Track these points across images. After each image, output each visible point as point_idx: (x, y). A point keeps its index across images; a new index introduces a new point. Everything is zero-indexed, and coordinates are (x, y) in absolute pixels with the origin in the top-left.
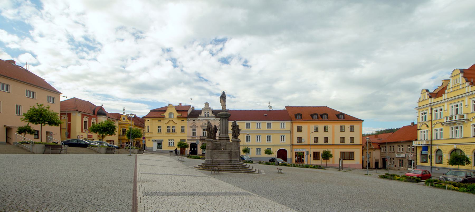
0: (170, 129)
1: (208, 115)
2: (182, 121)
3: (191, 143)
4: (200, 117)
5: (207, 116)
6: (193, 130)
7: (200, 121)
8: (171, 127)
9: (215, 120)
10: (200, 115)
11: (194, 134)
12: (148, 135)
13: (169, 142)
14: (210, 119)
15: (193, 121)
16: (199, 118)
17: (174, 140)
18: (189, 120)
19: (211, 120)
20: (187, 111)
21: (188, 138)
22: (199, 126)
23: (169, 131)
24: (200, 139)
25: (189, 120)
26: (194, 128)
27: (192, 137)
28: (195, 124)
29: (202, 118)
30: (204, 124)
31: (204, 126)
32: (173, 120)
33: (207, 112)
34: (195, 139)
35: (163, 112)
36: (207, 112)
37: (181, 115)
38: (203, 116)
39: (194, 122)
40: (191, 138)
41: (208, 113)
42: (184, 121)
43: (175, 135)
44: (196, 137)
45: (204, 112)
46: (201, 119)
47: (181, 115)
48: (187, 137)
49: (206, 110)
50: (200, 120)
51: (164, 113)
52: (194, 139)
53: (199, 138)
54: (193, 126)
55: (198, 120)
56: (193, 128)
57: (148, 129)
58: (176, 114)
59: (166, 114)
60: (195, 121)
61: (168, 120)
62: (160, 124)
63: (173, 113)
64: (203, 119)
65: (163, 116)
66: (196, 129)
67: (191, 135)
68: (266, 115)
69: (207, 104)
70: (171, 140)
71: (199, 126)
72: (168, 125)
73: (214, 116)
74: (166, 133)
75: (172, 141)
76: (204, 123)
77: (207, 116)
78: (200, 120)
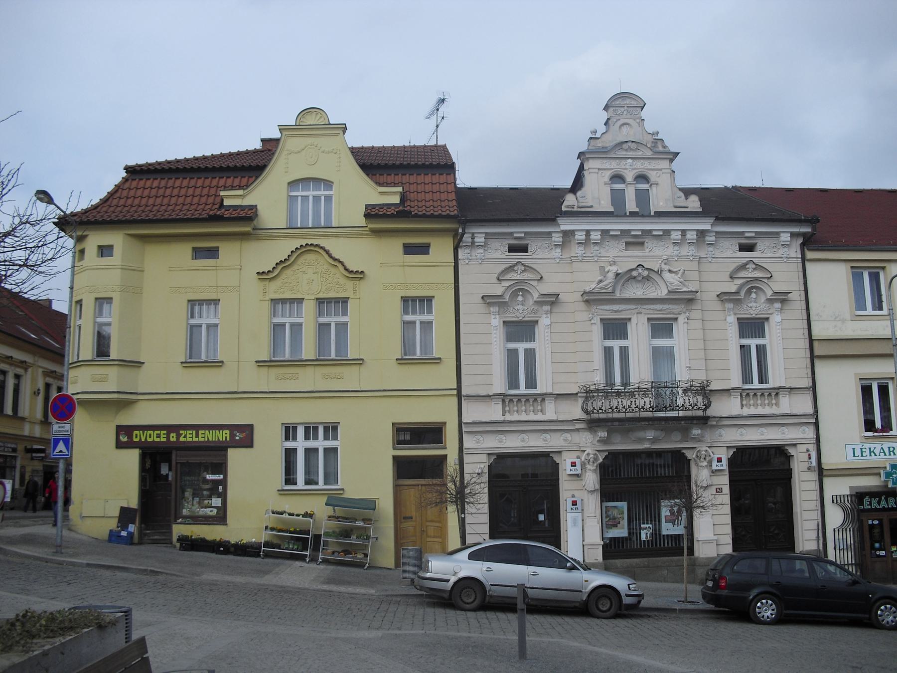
0: (297, 328)
1: (643, 198)
2: (409, 249)
5: (631, 205)
7: (576, 251)
8: (309, 308)
9: (711, 238)
12: (102, 380)
13: (290, 454)
14: (667, 233)
15: (512, 249)
16: (566, 225)
17: (331, 430)
18: (480, 239)
21: (472, 412)
22: (571, 297)
24: (583, 416)
25: (480, 239)
26: (520, 311)
27: (505, 399)
29: (597, 226)
30: (611, 276)
31: (618, 295)
33: (629, 177)
36: (629, 177)
37: (403, 199)
38: (596, 209)
40: (494, 412)
41: (642, 178)
42: (424, 249)
43: (350, 378)
44: (544, 396)
45: (607, 175)
46: (588, 233)
47: (396, 200)
48: (459, 396)
49: (622, 153)
53: (574, 410)
54: (515, 294)
55: (557, 238)
56: (510, 317)
60: (524, 249)
63: (328, 184)
64: (605, 233)
65: (235, 207)
66: (544, 321)
67: (499, 385)
70: (311, 431)
71: (571, 297)
74: (260, 363)
75: (321, 444)
76: (614, 269)
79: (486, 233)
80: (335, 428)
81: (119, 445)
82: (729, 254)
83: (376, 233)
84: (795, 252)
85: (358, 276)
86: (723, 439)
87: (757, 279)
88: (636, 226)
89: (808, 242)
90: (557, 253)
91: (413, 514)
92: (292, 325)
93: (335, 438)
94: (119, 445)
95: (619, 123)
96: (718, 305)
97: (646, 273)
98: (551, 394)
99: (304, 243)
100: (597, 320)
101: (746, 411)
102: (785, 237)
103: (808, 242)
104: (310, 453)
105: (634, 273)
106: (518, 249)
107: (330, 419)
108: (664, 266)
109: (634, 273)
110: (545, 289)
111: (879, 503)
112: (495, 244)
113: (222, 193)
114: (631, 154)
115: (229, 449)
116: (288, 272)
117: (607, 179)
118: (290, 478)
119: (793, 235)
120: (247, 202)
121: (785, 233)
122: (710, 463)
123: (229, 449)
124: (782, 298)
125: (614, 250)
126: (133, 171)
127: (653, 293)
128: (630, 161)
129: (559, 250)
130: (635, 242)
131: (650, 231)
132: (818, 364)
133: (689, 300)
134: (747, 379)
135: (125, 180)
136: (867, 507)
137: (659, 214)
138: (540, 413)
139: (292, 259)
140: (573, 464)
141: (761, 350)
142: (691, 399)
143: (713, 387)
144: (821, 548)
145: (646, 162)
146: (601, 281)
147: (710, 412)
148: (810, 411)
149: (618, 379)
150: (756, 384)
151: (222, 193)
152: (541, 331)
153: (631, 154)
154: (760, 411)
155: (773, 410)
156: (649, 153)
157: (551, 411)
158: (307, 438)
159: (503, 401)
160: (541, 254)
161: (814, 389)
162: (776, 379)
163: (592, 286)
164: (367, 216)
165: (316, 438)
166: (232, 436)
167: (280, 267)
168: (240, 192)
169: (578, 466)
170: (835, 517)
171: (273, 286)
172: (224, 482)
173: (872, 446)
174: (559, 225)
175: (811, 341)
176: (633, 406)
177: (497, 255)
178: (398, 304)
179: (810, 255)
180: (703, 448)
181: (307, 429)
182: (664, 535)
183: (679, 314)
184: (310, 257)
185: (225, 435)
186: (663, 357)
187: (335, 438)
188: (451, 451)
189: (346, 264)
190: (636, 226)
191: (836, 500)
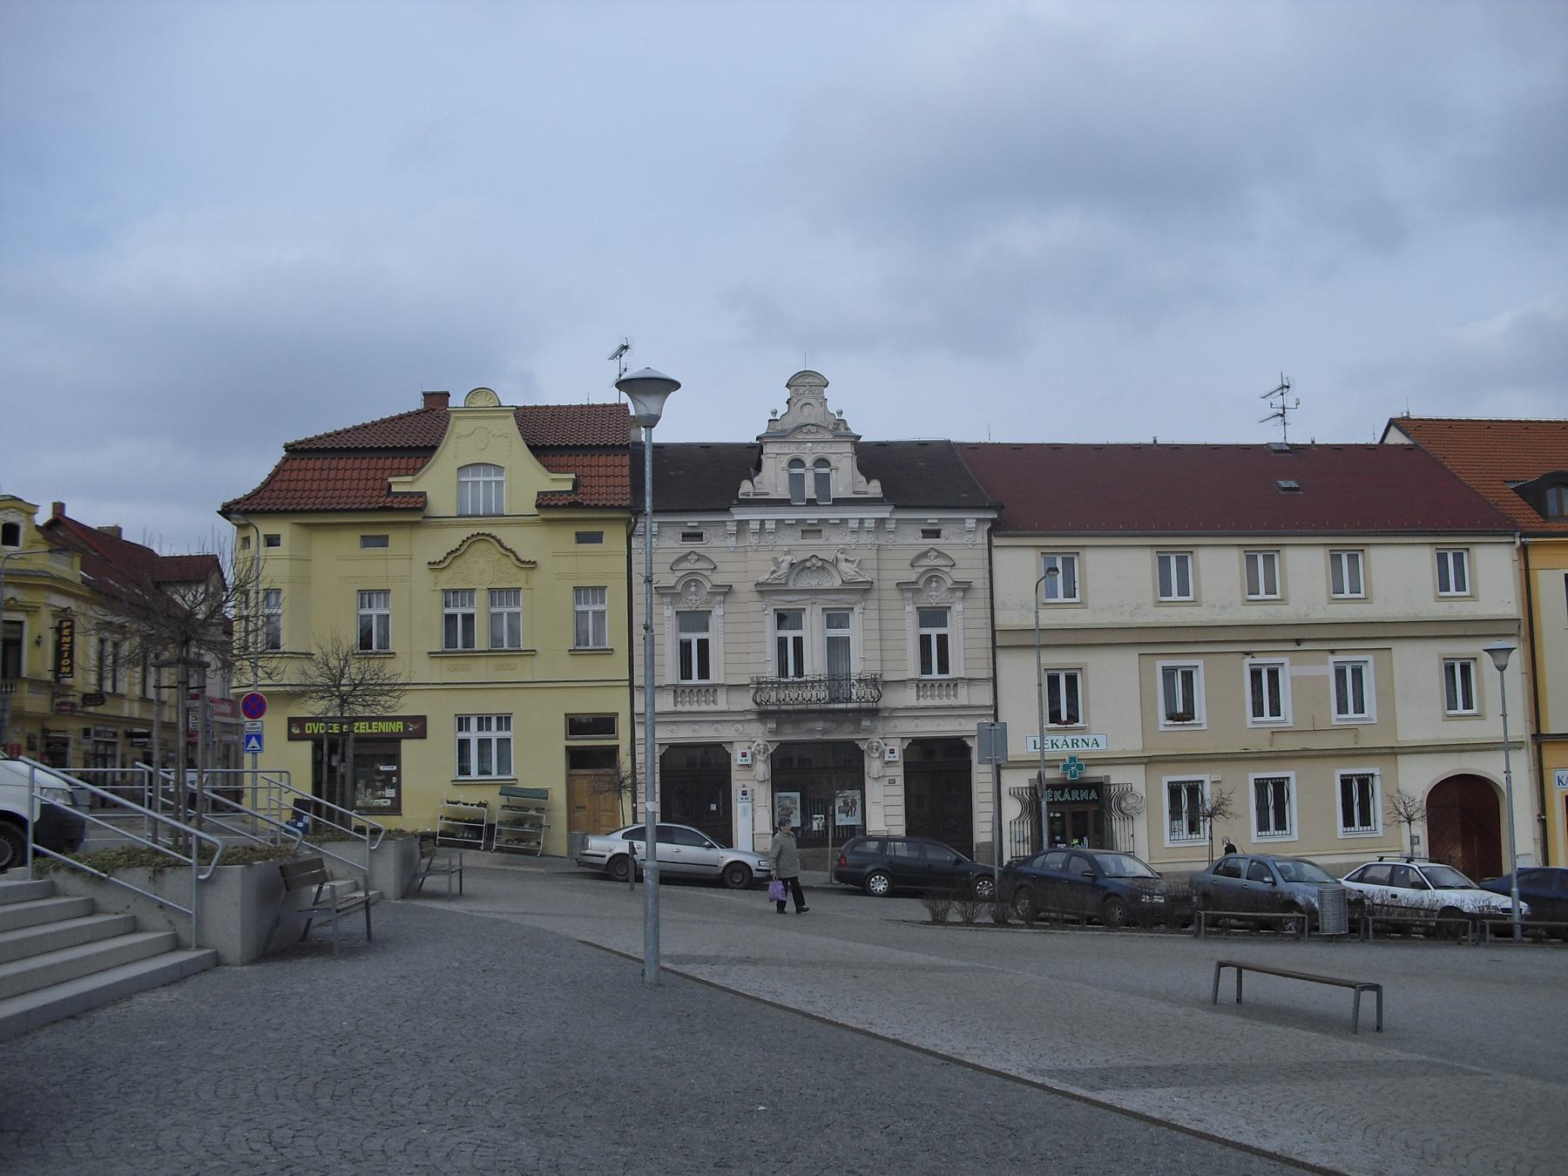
0: (468, 619)
1: (822, 482)
2: (582, 538)
3: (672, 747)
5: (810, 493)
6: (683, 629)
8: (481, 598)
9: (891, 526)
10: (746, 487)
11: (695, 658)
13: (463, 745)
14: (844, 521)
15: (686, 536)
16: (739, 514)
17: (504, 721)
19: (854, 524)
22: (744, 588)
28: (699, 565)
29: (771, 515)
30: (785, 566)
31: (791, 586)
32: (494, 531)
33: (809, 463)
34: (704, 707)
36: (809, 463)
37: (576, 484)
39: (691, 545)
41: (822, 462)
42: (596, 538)
43: (522, 670)
44: (715, 687)
45: (785, 460)
46: (762, 522)
47: (569, 487)
48: (631, 686)
49: (800, 437)
50: (755, 526)
51: (414, 471)
52: (695, 708)
53: (745, 702)
54: (687, 585)
55: (732, 528)
56: (683, 608)
60: (699, 536)
62: (373, 567)
63: (499, 469)
64: (779, 522)
65: (404, 494)
66: (718, 611)
68: (1293, 484)
69: (806, 384)
70: (484, 722)
71: (744, 588)
72: (451, 579)
73: (875, 489)
75: (494, 734)
76: (789, 558)
79: (659, 523)
80: (508, 719)
81: (292, 737)
82: (911, 540)
83: (546, 521)
84: (981, 538)
85: (531, 565)
86: (897, 730)
87: (935, 569)
88: (812, 515)
89: (996, 529)
90: (732, 541)
91: (587, 804)
92: (464, 616)
93: (508, 728)
94: (292, 737)
95: (801, 403)
96: (896, 595)
97: (820, 564)
98: (723, 685)
100: (770, 611)
101: (923, 703)
102: (971, 524)
103: (996, 529)
104: (484, 744)
105: (808, 564)
106: (693, 536)
108: (839, 555)
109: (808, 564)
110: (718, 579)
111: (1062, 796)
112: (668, 532)
113: (390, 480)
114: (810, 437)
115: (402, 741)
116: (460, 561)
117: (785, 464)
118: (464, 770)
119: (979, 520)
120: (415, 489)
121: (970, 519)
122: (882, 754)
123: (402, 741)
124: (965, 588)
125: (791, 539)
126: (294, 450)
127: (827, 585)
128: (809, 445)
129: (733, 539)
130: (811, 530)
132: (998, 652)
133: (865, 590)
135: (285, 460)
137: (839, 502)
138: (712, 704)
139: (463, 549)
140: (744, 755)
141: (942, 640)
142: (868, 692)
143: (888, 677)
145: (827, 445)
146: (774, 572)
147: (881, 704)
148: (989, 701)
149: (791, 671)
151: (390, 480)
152: (715, 622)
154: (937, 702)
155: (952, 702)
156: (829, 437)
157: (723, 702)
158: (480, 728)
159: (675, 691)
160: (715, 542)
161: (994, 680)
162: (956, 670)
163: (763, 578)
164: (538, 506)
165: (489, 729)
166: (406, 727)
167: (451, 557)
168: (409, 479)
169: (749, 757)
170: (1012, 809)
171: (444, 576)
172: (398, 773)
173: (1055, 738)
174: (732, 515)
175: (994, 631)
176: (800, 698)
177: (671, 544)
178: (571, 594)
179: (996, 541)
180: (875, 739)
181: (480, 720)
182: (838, 826)
183: (854, 604)
184: (481, 546)
185: (397, 727)
186: (837, 649)
187: (508, 728)
188: (623, 743)
189: (518, 554)
190: (812, 515)
191: (1016, 793)
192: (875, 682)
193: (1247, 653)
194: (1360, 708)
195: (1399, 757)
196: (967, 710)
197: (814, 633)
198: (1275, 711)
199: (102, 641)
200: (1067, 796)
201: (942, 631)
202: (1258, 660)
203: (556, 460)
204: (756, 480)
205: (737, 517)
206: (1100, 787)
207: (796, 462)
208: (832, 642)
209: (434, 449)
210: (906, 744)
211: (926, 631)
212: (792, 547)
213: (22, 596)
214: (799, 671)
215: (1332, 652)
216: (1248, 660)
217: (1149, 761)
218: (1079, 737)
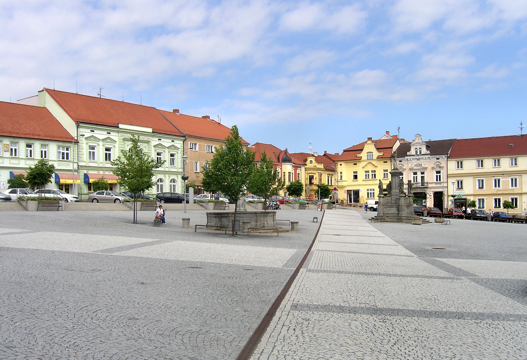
1: (420, 151)
2: (384, 162)
4: (408, 156)
5: (418, 153)
8: (370, 172)
9: (431, 158)
10: (408, 153)
12: (341, 184)
13: (368, 193)
16: (406, 158)
17: (374, 190)
19: (424, 158)
20: (392, 148)
23: (367, 176)
28: (401, 166)
29: (411, 157)
31: (414, 168)
33: (418, 149)
35: (359, 152)
36: (418, 149)
42: (386, 162)
55: (406, 160)
57: (341, 176)
58: (376, 154)
59: (364, 155)
61: (365, 163)
63: (372, 153)
64: (413, 158)
70: (371, 190)
73: (428, 152)
75: (372, 192)
77: (418, 153)
78: (409, 159)
84: (446, 159)
88: (418, 157)
89: (448, 157)
99: (369, 162)
100: (412, 172)
101: (436, 186)
102: (444, 157)
103: (448, 157)
107: (373, 188)
113: (357, 155)
114: (418, 145)
117: (414, 149)
121: (444, 156)
124: (443, 167)
126: (344, 151)
130: (418, 159)
131: (420, 158)
132: (448, 178)
134: (437, 180)
135: (343, 152)
136: (457, 201)
144: (447, 207)
148: (447, 186)
150: (438, 181)
151: (357, 155)
153: (418, 145)
154: (438, 186)
160: (404, 162)
162: (442, 181)
163: (410, 167)
170: (450, 203)
171: (364, 169)
186: (423, 178)
191: (450, 200)
192: (427, 183)
193: (493, 177)
194: (516, 186)
195: (523, 195)
196: (443, 187)
197: (419, 175)
198: (499, 186)
199: (328, 177)
200: (460, 201)
201: (440, 174)
202: (495, 178)
203: (379, 150)
204: (410, 152)
205: (406, 158)
206: (465, 199)
207: (416, 149)
208: (422, 177)
209: (363, 150)
210: (433, 193)
211: (437, 174)
212: (415, 162)
213: (313, 172)
214: (416, 182)
215: (510, 176)
216: (493, 178)
217: (474, 195)
218: (462, 191)
